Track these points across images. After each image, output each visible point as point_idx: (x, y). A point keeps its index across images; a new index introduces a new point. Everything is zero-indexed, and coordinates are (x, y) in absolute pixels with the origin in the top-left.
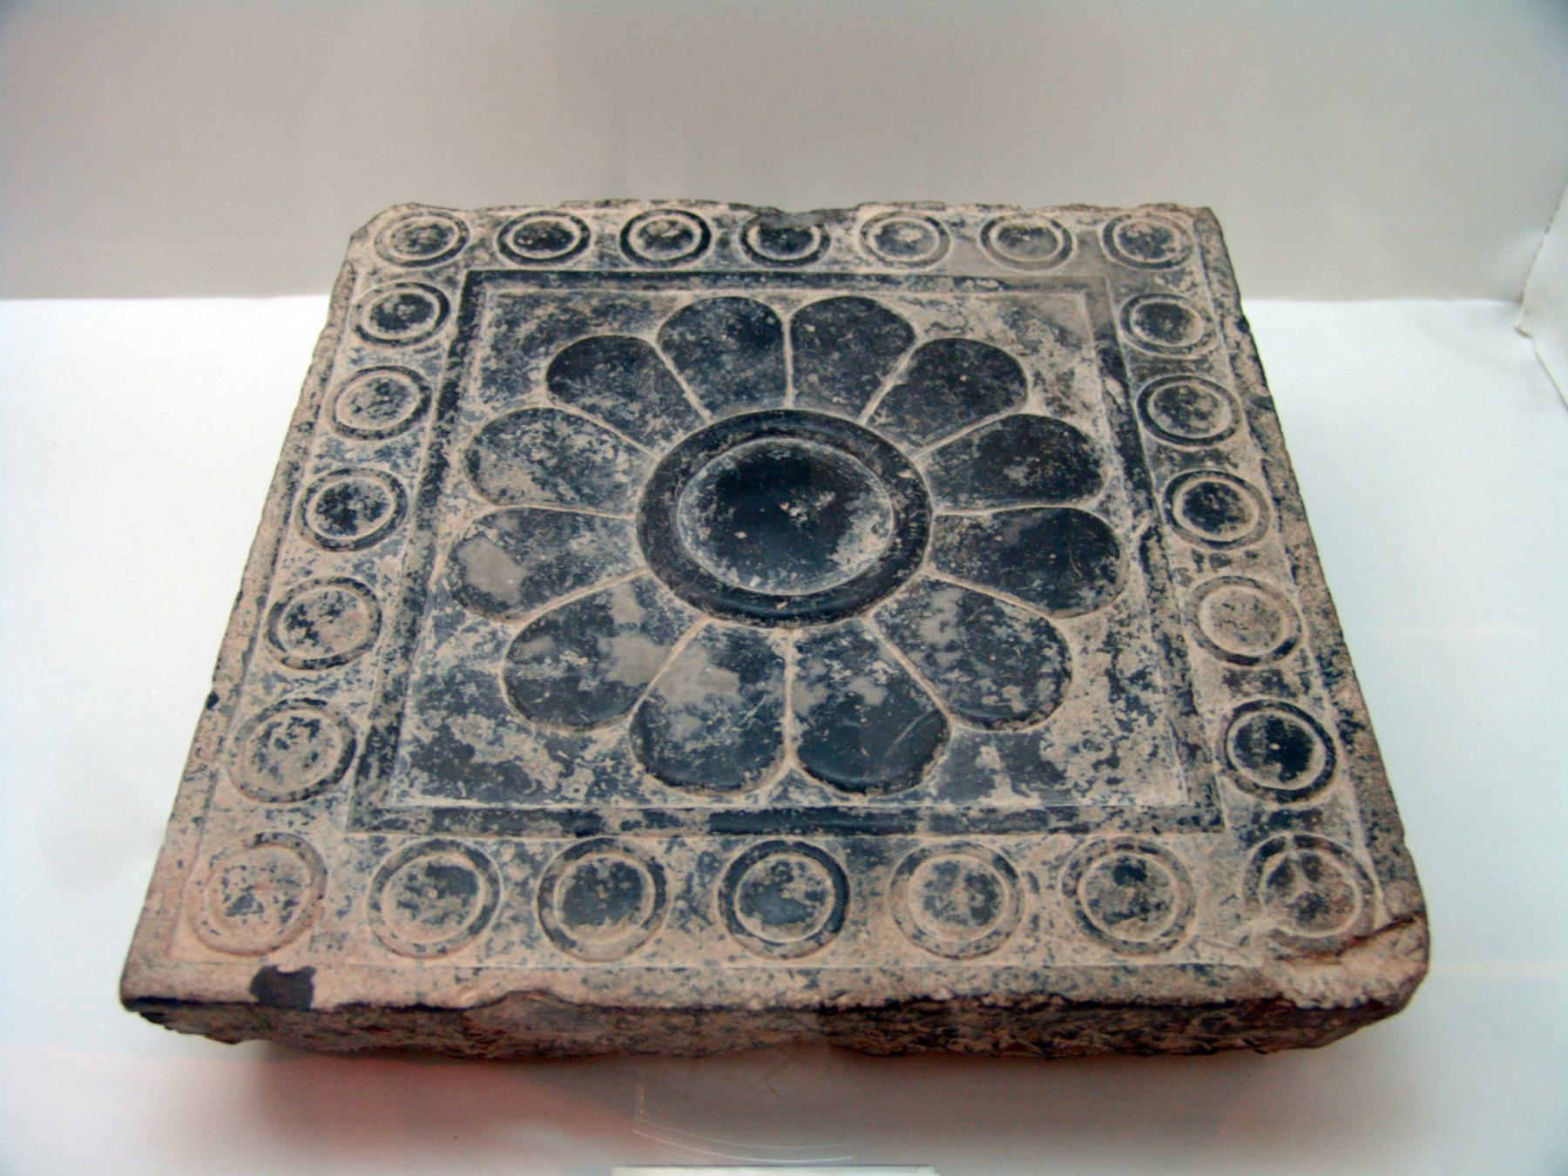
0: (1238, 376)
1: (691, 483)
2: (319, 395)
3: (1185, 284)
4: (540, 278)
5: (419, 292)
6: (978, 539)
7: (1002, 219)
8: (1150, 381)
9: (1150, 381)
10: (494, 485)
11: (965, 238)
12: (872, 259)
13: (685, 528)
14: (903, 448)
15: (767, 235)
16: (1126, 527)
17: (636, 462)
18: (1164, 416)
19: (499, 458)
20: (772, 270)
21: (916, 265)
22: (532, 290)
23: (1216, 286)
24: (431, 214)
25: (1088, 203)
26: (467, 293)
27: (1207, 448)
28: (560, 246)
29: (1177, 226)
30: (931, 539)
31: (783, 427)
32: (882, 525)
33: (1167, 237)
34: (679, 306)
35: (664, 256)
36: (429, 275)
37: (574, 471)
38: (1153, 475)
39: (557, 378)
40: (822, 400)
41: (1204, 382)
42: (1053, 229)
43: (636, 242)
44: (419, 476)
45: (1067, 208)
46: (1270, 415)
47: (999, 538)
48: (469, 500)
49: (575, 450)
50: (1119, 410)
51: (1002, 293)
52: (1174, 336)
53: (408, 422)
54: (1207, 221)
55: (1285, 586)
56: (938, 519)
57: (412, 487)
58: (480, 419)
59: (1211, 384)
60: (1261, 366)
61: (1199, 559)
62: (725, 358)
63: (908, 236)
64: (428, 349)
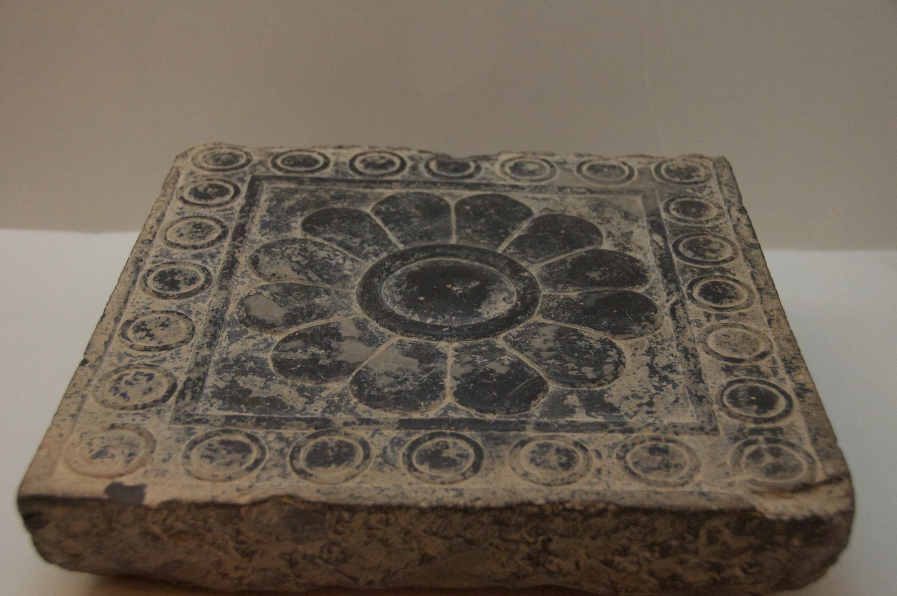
0: (737, 233)
1: (391, 276)
2: (155, 227)
3: (705, 193)
4: (300, 181)
5: (221, 183)
6: (569, 304)
7: (590, 161)
8: (681, 236)
9: (681, 236)
10: (268, 271)
11: (566, 169)
12: (507, 178)
13: (387, 296)
14: (524, 264)
15: (441, 165)
16: (662, 300)
17: (356, 265)
18: (688, 251)
19: (271, 259)
20: (444, 181)
21: (535, 181)
22: (292, 186)
23: (726, 193)
24: (228, 148)
25: (645, 153)
26: (252, 185)
27: (716, 266)
28: (311, 165)
29: (702, 165)
30: (539, 305)
31: (449, 252)
32: (510, 298)
33: (696, 170)
34: (385, 196)
35: (376, 172)
36: (228, 176)
37: (318, 268)
38: (680, 278)
39: (308, 225)
40: (472, 240)
41: (715, 236)
42: (623, 166)
43: (358, 165)
44: (220, 267)
45: (632, 156)
46: (757, 251)
47: (582, 304)
48: (252, 280)
49: (320, 258)
50: (660, 248)
51: (588, 195)
52: (698, 215)
53: (212, 243)
54: (722, 163)
55: (765, 329)
56: (544, 296)
57: (215, 272)
58: (258, 243)
59: (720, 237)
60: (753, 229)
61: (708, 316)
62: (413, 219)
63: (531, 167)
64: (226, 210)
